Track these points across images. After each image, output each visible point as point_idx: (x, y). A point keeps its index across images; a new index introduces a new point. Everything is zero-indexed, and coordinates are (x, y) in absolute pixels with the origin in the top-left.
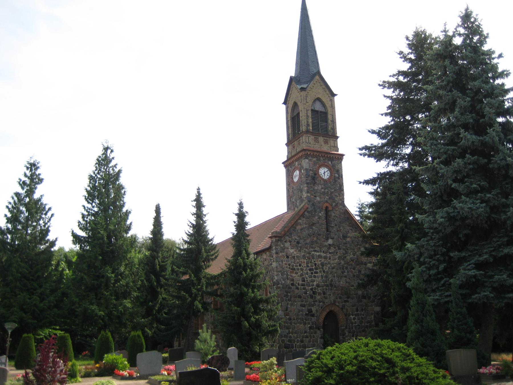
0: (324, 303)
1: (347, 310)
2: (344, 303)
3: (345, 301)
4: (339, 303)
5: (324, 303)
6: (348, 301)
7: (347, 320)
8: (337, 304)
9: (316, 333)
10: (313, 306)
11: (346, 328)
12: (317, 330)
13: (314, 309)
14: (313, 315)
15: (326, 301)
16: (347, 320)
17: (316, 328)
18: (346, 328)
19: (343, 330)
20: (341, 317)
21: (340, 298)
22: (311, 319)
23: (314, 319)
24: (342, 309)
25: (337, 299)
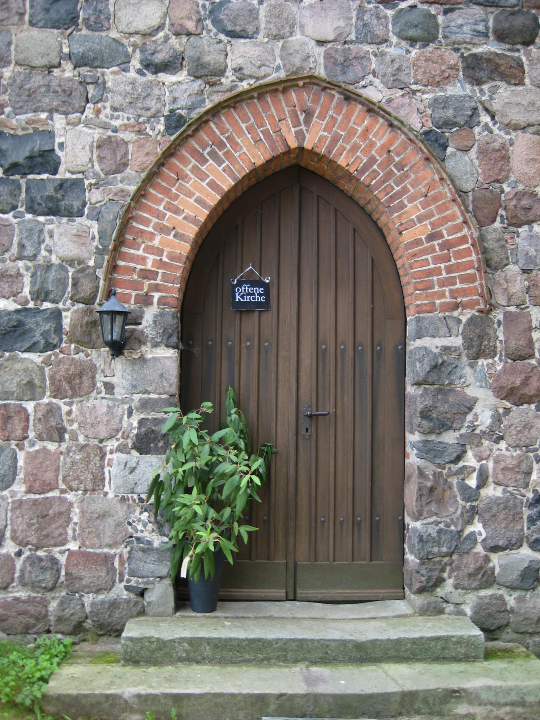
0: (207, 73)
1: (498, 158)
2: (458, 89)
3: (477, 69)
4: (396, 82)
5: (207, 73)
6: (513, 74)
7: (489, 265)
8: (375, 93)
9: (76, 383)
10: (73, 101)
11: (478, 346)
12: (100, 356)
13: (75, 145)
14: (60, 203)
15: (241, 53)
16: (489, 265)
17: (85, 337)
18: (478, 346)
19: (440, 369)
20: (417, 220)
21: (423, 34)
22: (37, 236)
23: (67, 240)
24: (434, 143)
25: (366, 35)
